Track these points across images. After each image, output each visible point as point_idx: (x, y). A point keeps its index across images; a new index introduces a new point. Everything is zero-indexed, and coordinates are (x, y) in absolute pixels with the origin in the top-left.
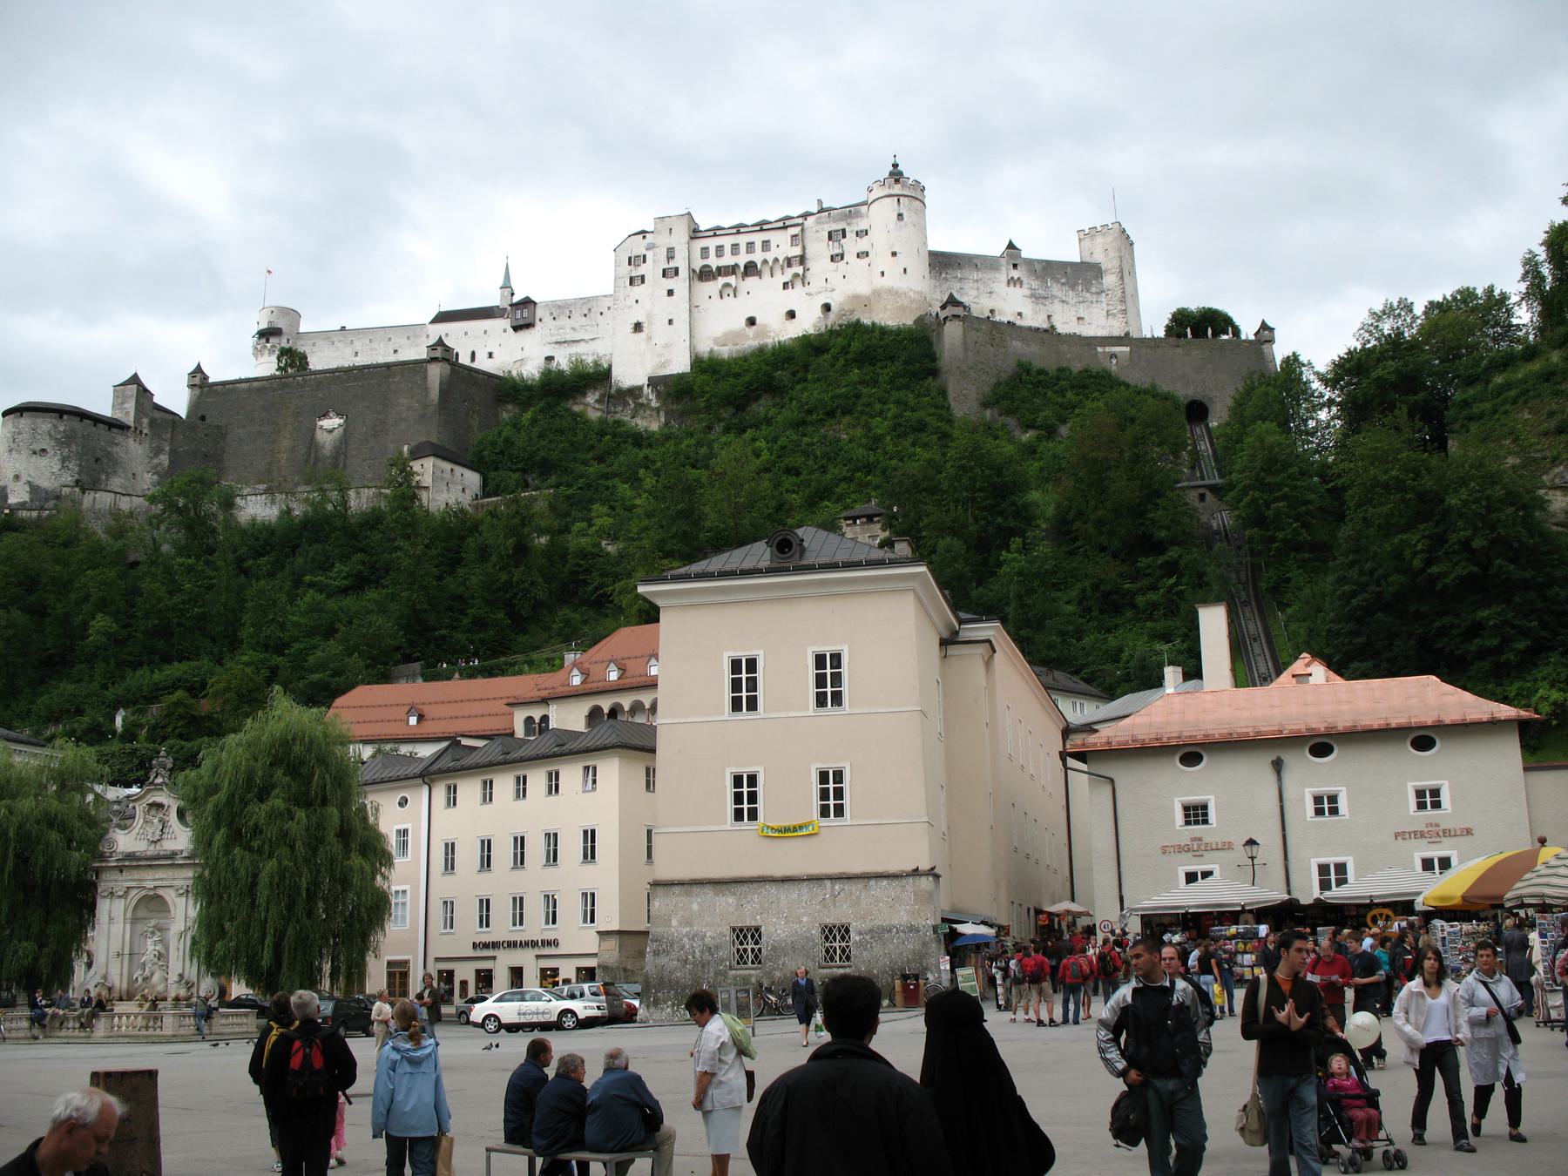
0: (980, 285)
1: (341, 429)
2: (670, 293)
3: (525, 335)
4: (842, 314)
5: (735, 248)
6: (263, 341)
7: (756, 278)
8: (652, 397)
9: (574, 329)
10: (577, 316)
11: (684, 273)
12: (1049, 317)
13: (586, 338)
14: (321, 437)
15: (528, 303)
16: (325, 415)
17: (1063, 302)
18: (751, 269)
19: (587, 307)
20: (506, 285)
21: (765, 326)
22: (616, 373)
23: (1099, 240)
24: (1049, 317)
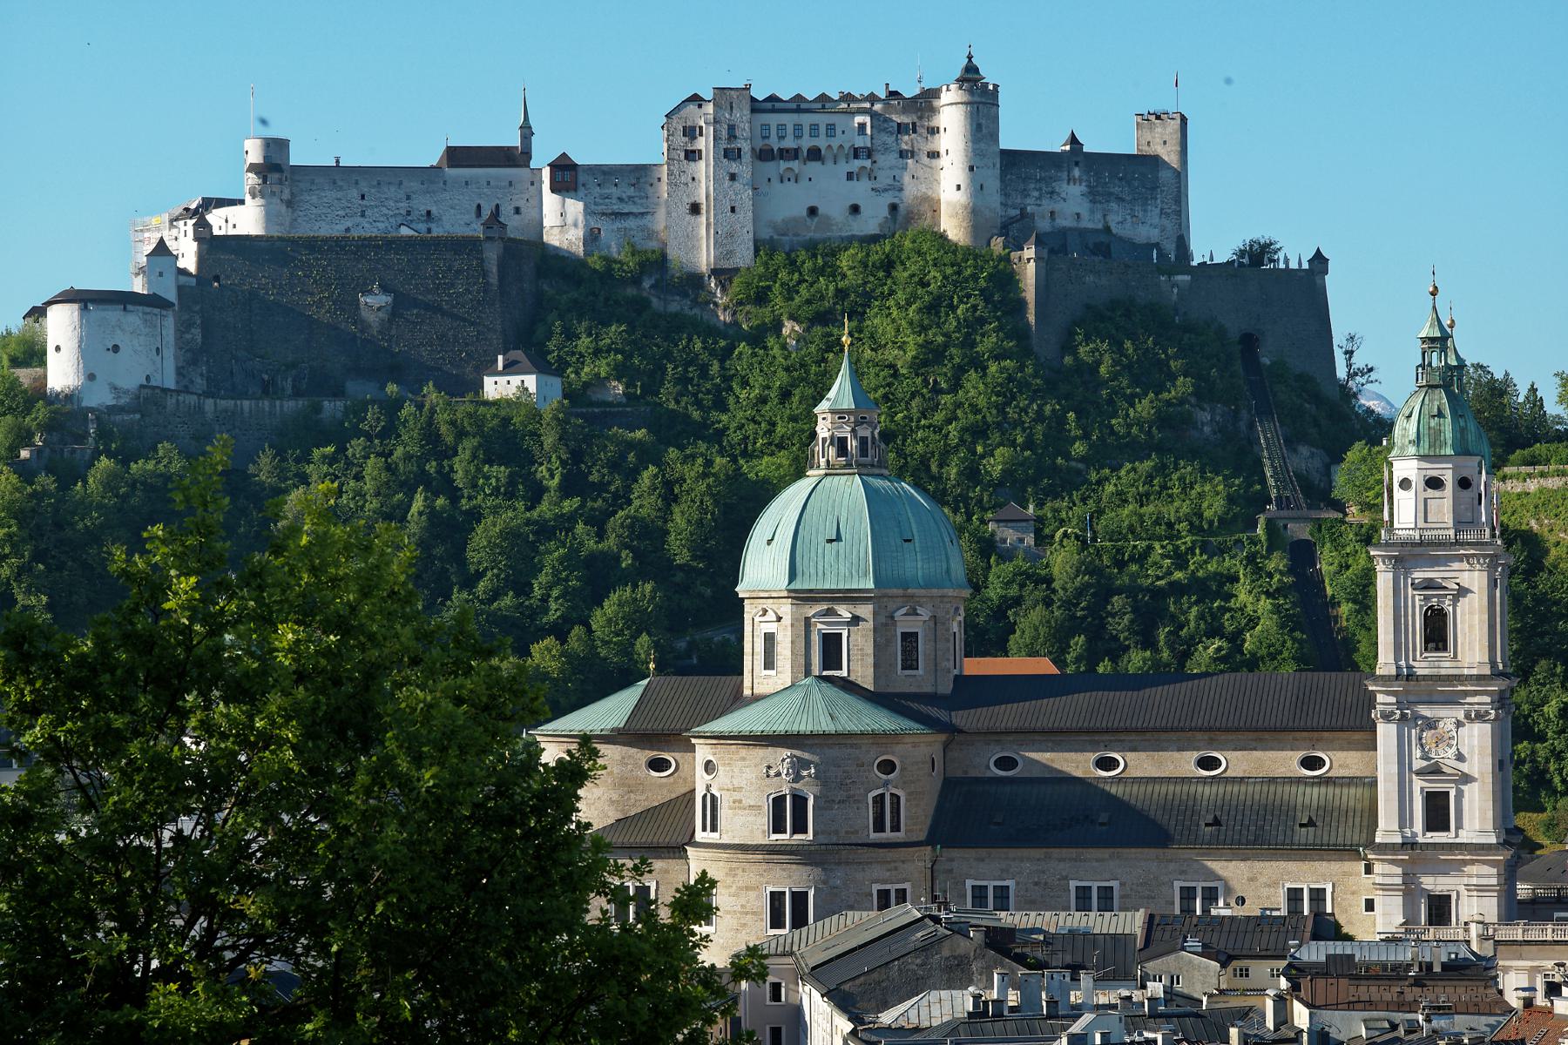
1: (389, 308)
2: (733, 177)
5: (798, 128)
7: (819, 163)
9: (620, 199)
11: (747, 156)
12: (1105, 216)
13: (635, 210)
14: (365, 313)
16: (370, 292)
17: (1120, 200)
18: (815, 154)
21: (828, 218)
22: (673, 253)
23: (1159, 130)
24: (1105, 216)
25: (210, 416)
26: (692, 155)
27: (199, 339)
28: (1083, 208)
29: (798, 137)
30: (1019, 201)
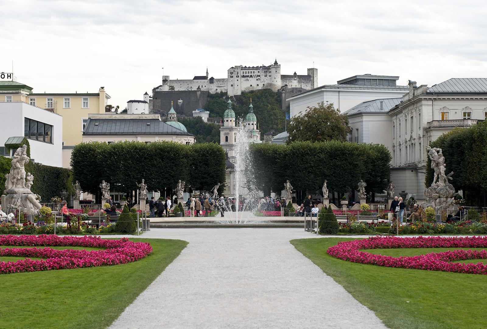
0: (289, 81)
2: (238, 80)
3: (212, 85)
5: (249, 72)
9: (220, 84)
10: (221, 82)
12: (301, 86)
14: (178, 103)
15: (212, 79)
16: (179, 100)
17: (303, 83)
18: (251, 76)
20: (207, 73)
22: (228, 93)
23: (311, 71)
24: (301, 86)
27: (152, 107)
30: (285, 83)
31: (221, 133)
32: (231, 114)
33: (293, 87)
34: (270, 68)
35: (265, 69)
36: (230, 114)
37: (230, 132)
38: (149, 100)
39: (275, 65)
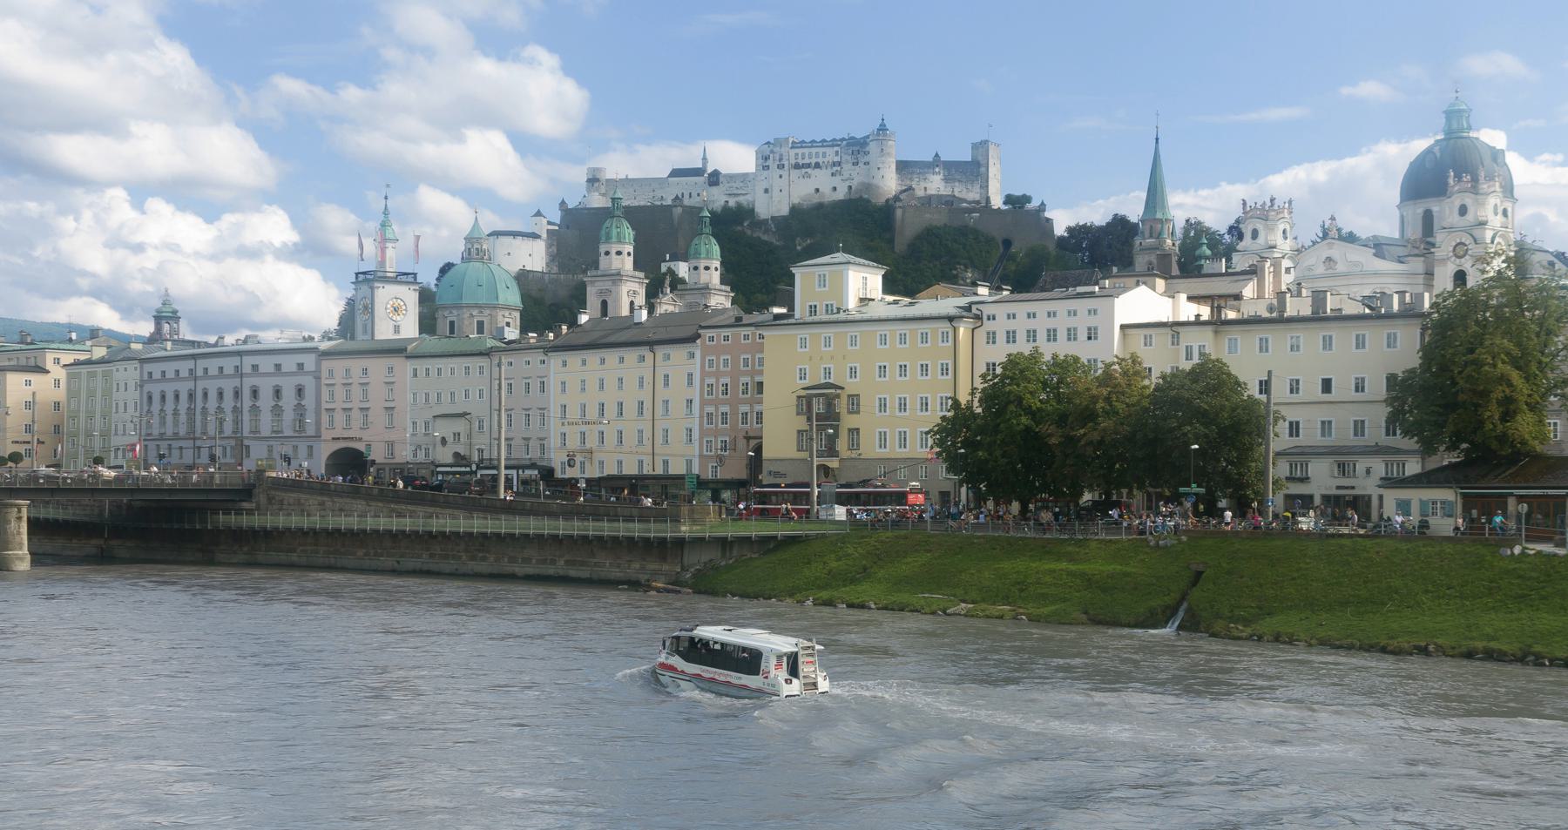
2: (781, 177)
4: (856, 193)
6: (591, 184)
8: (773, 226)
9: (737, 188)
13: (743, 192)
17: (959, 181)
18: (817, 166)
19: (746, 175)
20: (705, 159)
23: (980, 150)
25: (547, 281)
26: (766, 168)
27: (555, 251)
28: (943, 183)
29: (810, 158)
30: (908, 182)
31: (588, 289)
32: (618, 233)
33: (930, 192)
34: (868, 140)
35: (853, 145)
36: (614, 232)
37: (613, 288)
38: (548, 230)
39: (878, 134)
